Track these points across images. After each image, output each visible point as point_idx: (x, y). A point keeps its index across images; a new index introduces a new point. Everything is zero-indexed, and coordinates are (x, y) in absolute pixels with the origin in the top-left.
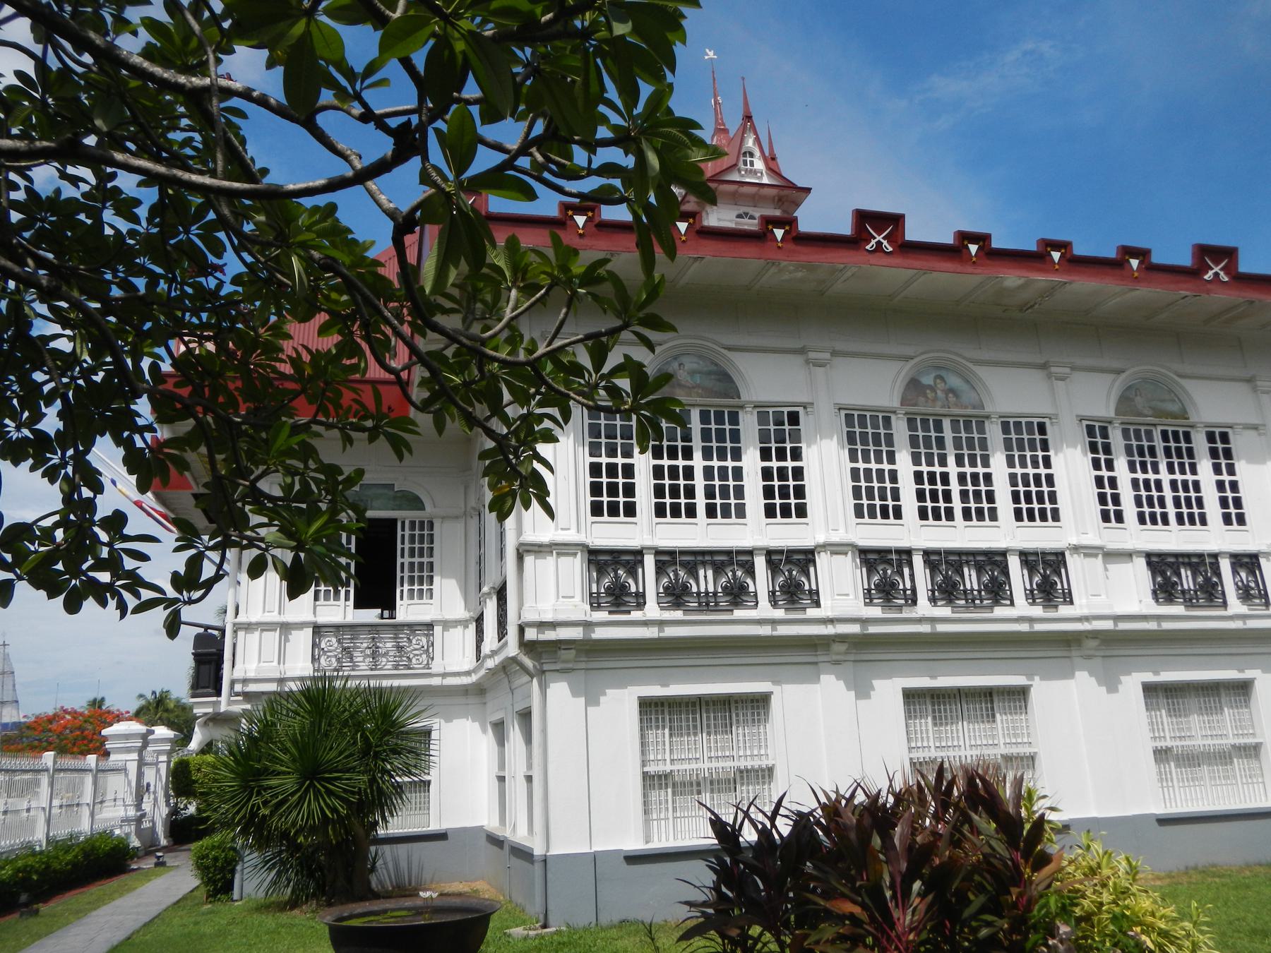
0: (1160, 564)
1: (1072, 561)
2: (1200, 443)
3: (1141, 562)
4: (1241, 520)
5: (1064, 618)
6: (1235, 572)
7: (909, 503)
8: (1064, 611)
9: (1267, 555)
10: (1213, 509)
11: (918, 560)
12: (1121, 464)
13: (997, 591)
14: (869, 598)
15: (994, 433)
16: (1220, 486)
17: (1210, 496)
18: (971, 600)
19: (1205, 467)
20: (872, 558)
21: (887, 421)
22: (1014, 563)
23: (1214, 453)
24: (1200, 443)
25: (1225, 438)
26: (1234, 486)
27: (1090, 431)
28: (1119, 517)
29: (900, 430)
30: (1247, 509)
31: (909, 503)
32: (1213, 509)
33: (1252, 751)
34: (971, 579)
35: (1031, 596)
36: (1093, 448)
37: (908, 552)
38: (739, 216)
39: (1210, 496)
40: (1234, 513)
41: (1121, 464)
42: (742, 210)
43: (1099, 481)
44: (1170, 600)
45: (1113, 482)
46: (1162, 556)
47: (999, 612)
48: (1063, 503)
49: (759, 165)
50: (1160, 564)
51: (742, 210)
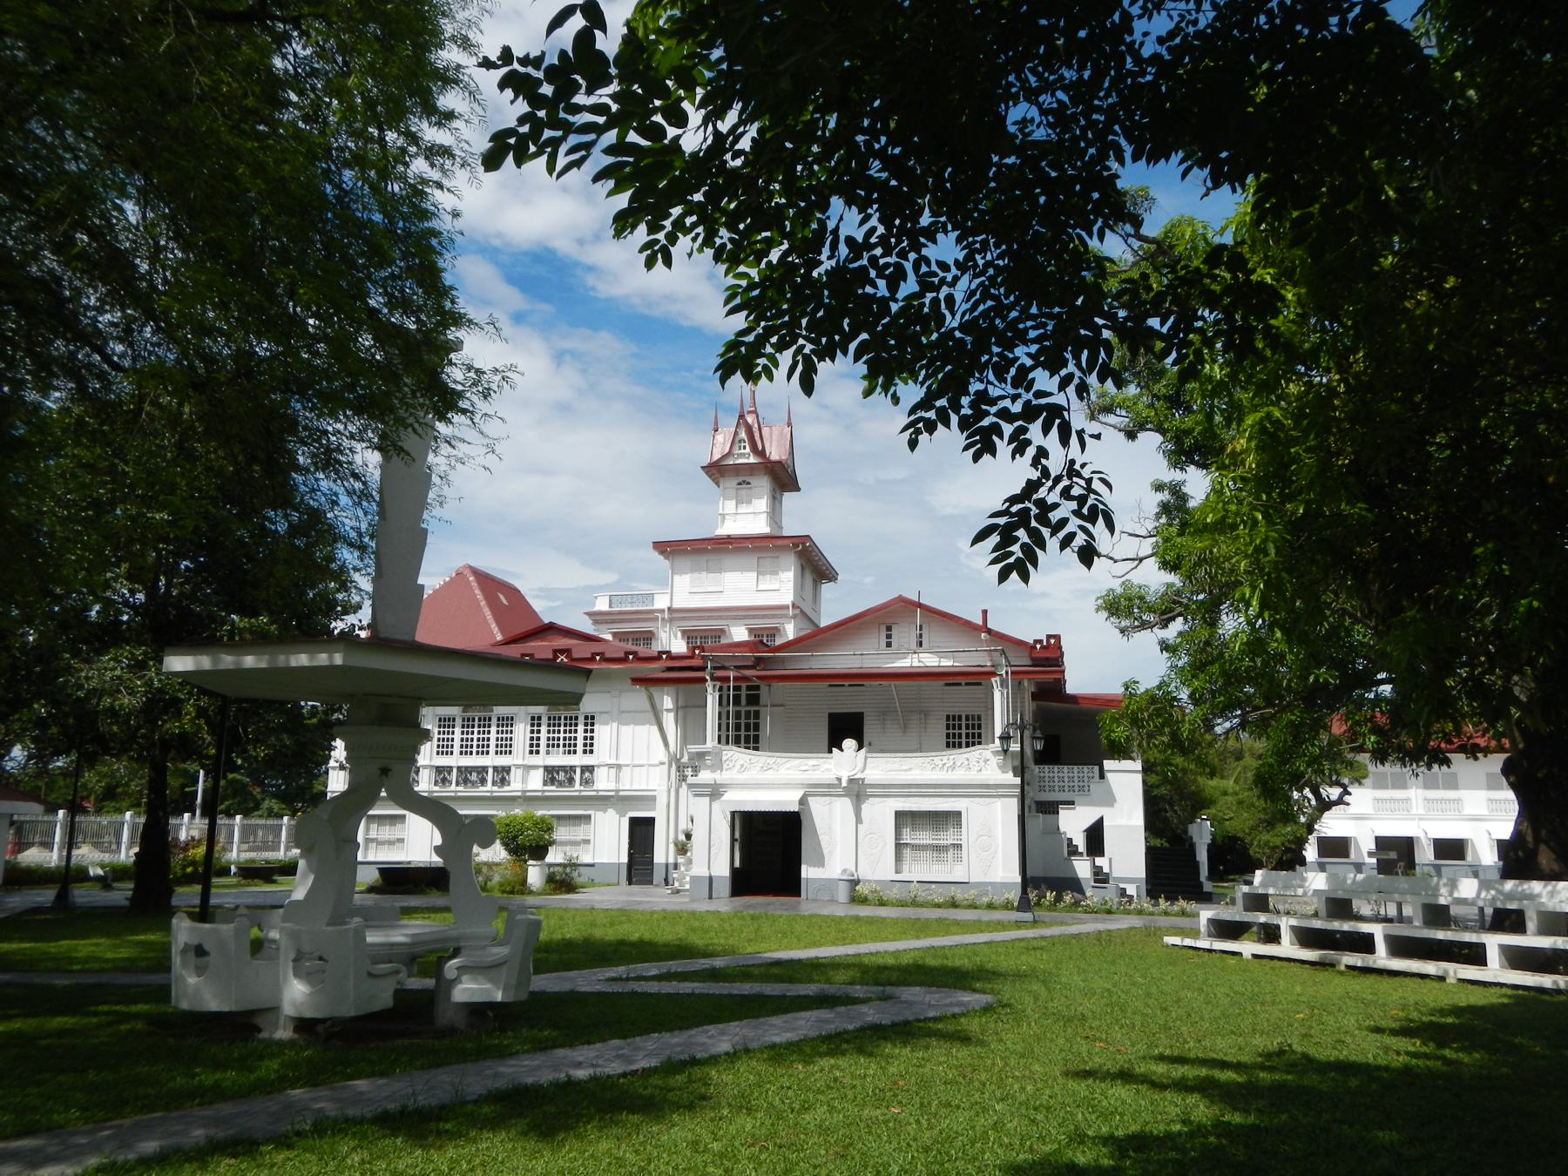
0: (551, 773)
1: (513, 769)
2: (581, 720)
3: (542, 770)
4: (591, 752)
5: (506, 791)
6: (582, 772)
7: (456, 749)
8: (506, 788)
9: (599, 766)
10: (580, 748)
11: (455, 770)
12: (544, 729)
13: (483, 781)
14: (436, 783)
15: (494, 721)
16: (586, 738)
17: (580, 742)
18: (473, 784)
19: (581, 728)
20: (439, 770)
21: (454, 720)
22: (490, 771)
23: (586, 725)
24: (581, 720)
25: (593, 718)
26: (592, 738)
27: (533, 719)
28: (538, 752)
29: (459, 722)
30: (594, 748)
31: (456, 749)
32: (580, 748)
33: (587, 842)
34: (474, 777)
35: (494, 783)
36: (532, 725)
37: (451, 767)
38: (740, 484)
39: (580, 742)
40: (589, 748)
41: (544, 729)
42: (741, 479)
43: (532, 739)
44: (552, 784)
45: (538, 739)
46: (553, 767)
47: (482, 789)
48: (514, 749)
49: (748, 450)
50: (551, 773)
51: (741, 479)
